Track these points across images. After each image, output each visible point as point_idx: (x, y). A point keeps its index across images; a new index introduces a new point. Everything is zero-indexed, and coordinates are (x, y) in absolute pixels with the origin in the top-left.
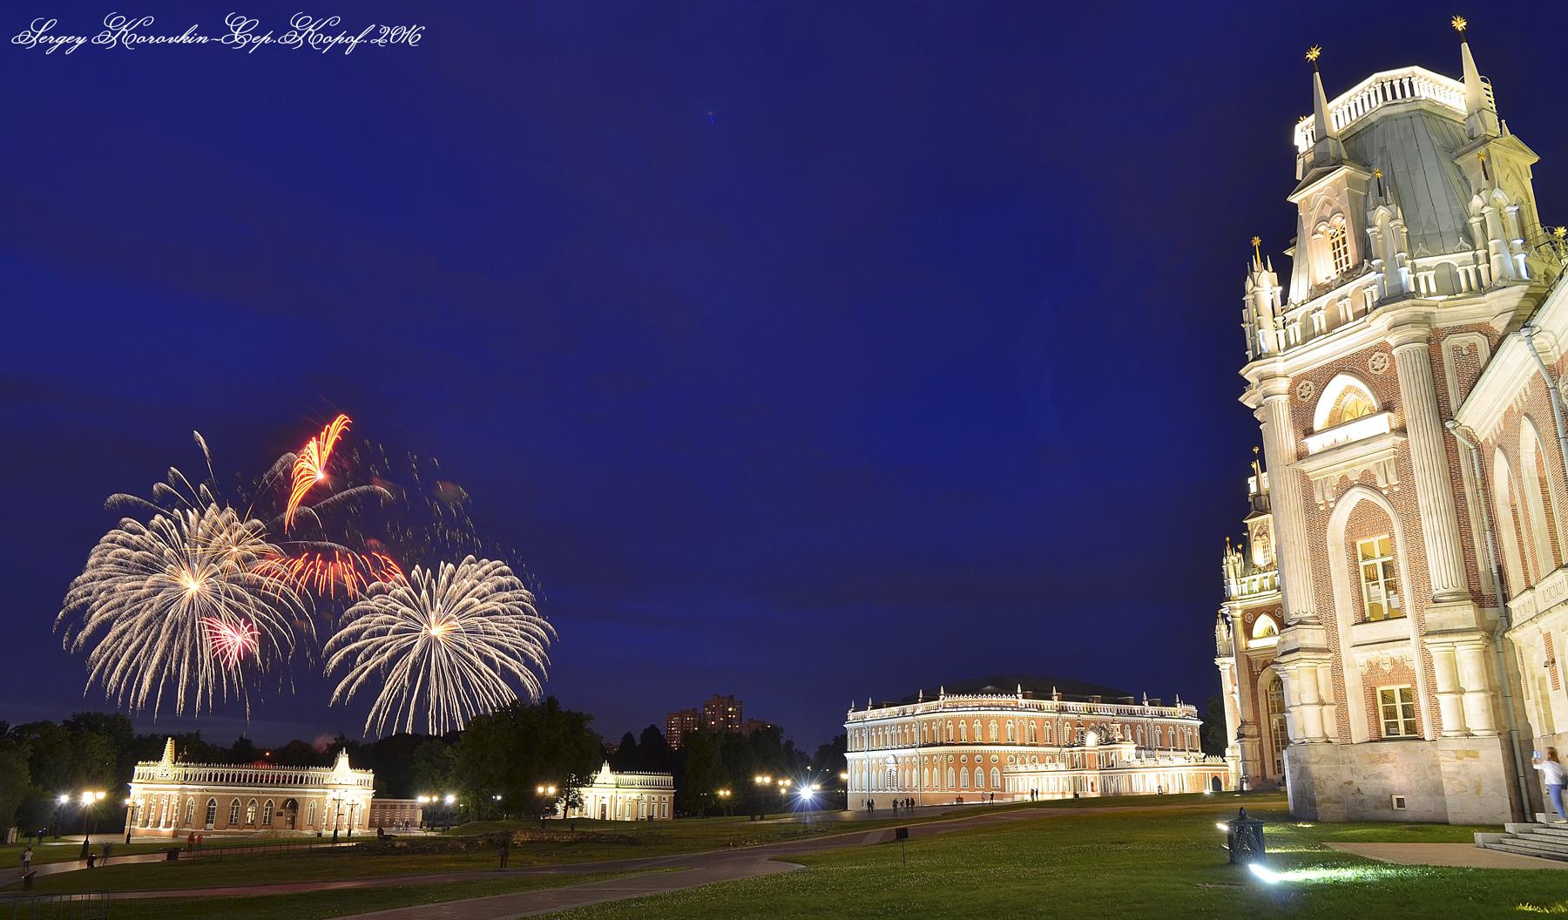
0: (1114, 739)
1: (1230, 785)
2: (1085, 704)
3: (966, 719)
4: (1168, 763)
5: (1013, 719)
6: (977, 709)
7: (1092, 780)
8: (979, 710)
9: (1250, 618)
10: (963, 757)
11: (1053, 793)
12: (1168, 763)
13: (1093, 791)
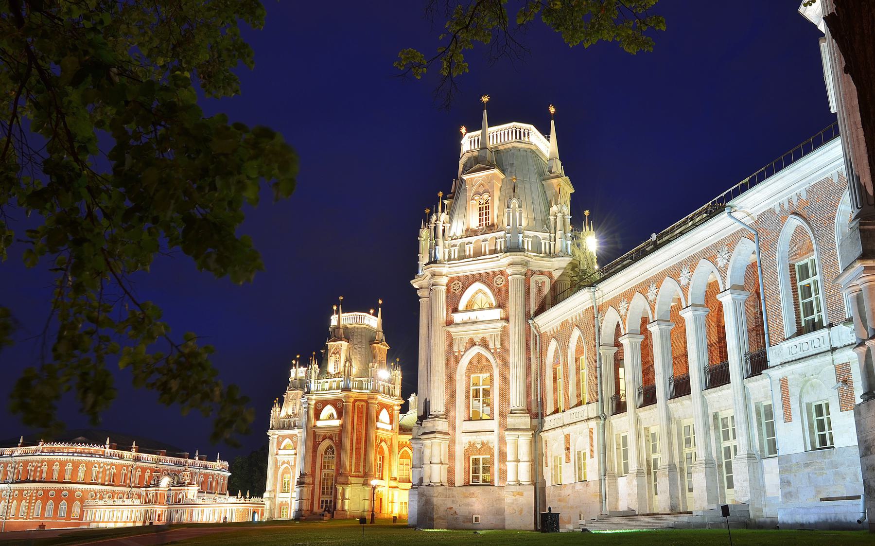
0: (184, 483)
1: (263, 517)
2: (154, 456)
3: (59, 461)
4: (223, 501)
5: (99, 464)
6: (71, 454)
7: (160, 512)
8: (73, 456)
9: (319, 406)
10: (51, 493)
11: (125, 522)
12: (223, 501)
13: (158, 520)
